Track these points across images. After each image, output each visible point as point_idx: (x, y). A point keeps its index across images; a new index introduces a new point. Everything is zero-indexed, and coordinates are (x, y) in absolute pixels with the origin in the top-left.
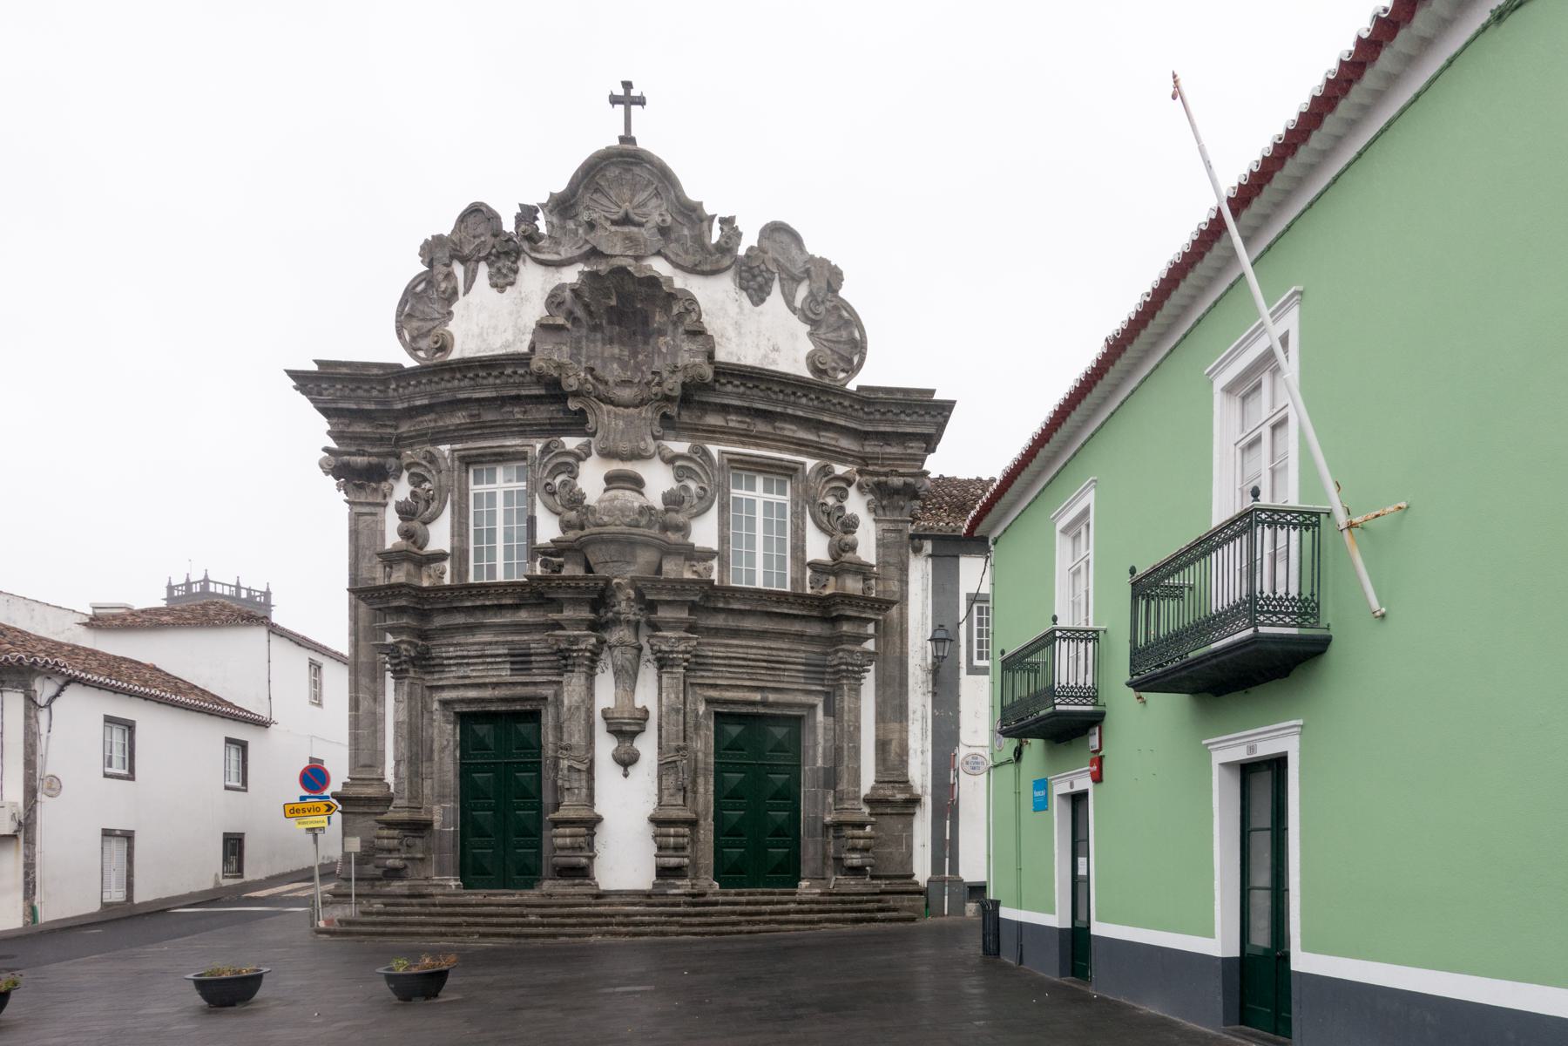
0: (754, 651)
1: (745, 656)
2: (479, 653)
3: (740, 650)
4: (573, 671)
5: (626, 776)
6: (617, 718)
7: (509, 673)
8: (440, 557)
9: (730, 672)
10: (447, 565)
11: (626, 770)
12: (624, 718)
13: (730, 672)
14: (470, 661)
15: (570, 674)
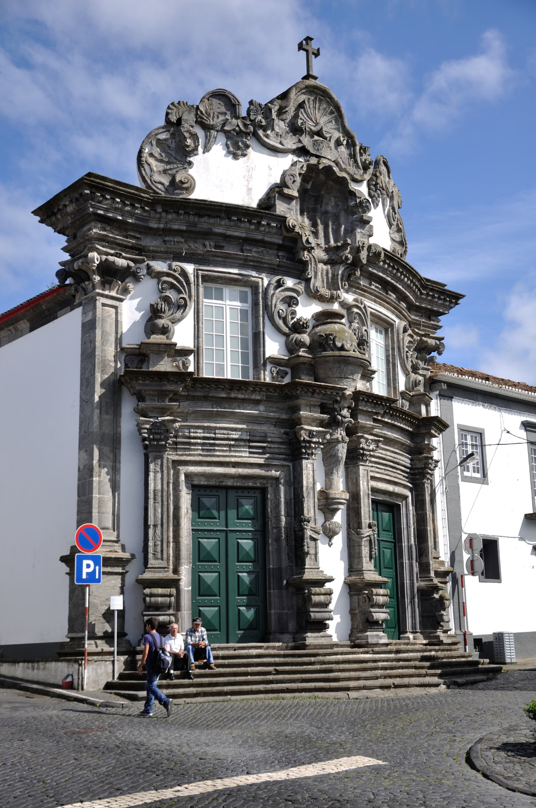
0: (389, 453)
1: (384, 456)
2: (226, 436)
3: (384, 452)
4: (308, 459)
5: (330, 545)
6: (338, 499)
7: (247, 455)
8: (185, 352)
9: (377, 468)
10: (191, 358)
11: (330, 541)
12: (342, 499)
13: (377, 468)
14: (217, 442)
15: (307, 461)
